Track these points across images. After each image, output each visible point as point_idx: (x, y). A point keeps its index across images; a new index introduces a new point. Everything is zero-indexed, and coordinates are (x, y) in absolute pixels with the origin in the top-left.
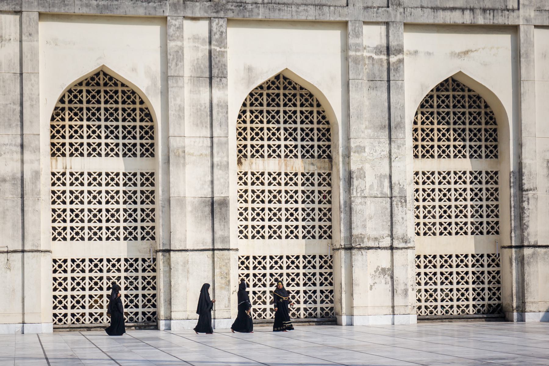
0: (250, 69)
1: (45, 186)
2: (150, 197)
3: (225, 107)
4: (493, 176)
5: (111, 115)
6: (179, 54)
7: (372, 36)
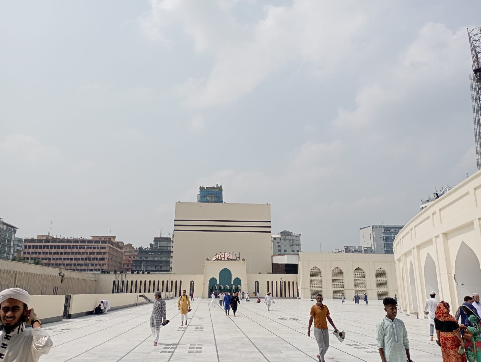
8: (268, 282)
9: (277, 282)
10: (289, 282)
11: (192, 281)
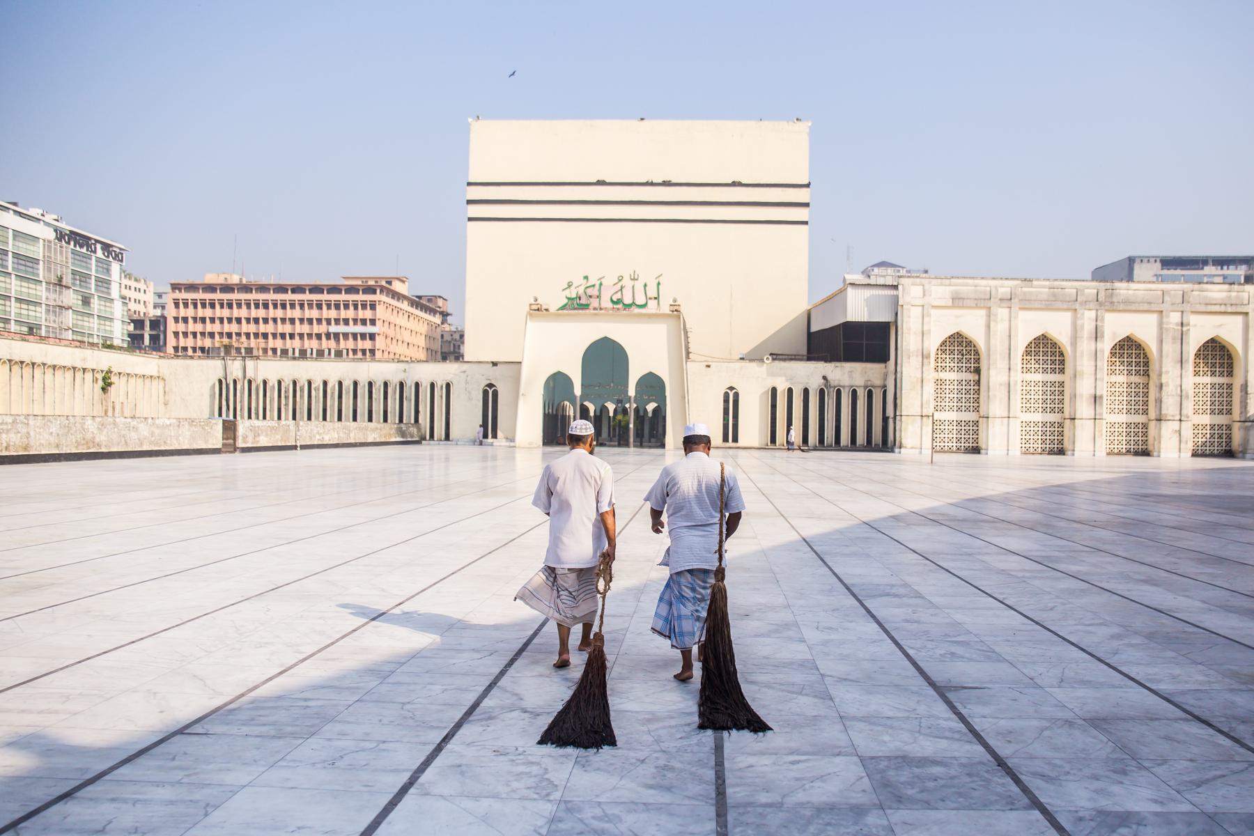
0: (1114, 334)
1: (1019, 388)
2: (1062, 393)
3: (1103, 351)
4: (1230, 386)
5: (1045, 354)
6: (1082, 326)
7: (1175, 318)
8: (774, 390)
9: (806, 391)
10: (854, 393)
11: (490, 385)
